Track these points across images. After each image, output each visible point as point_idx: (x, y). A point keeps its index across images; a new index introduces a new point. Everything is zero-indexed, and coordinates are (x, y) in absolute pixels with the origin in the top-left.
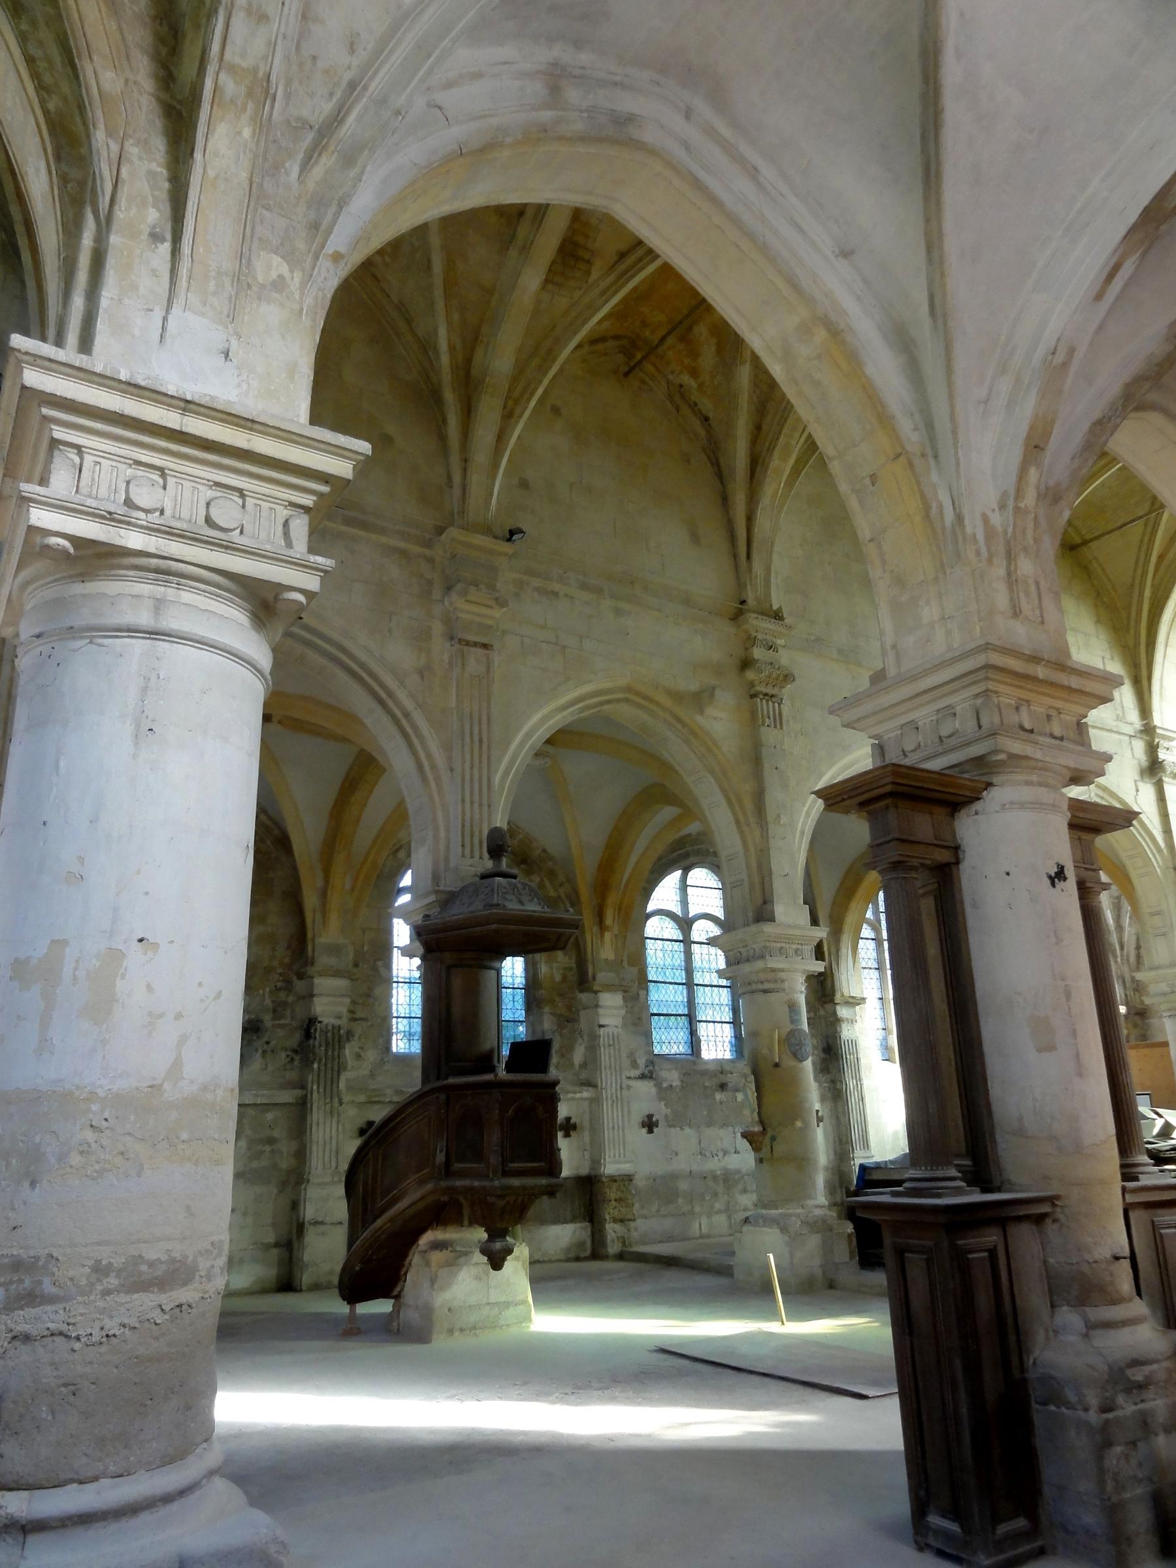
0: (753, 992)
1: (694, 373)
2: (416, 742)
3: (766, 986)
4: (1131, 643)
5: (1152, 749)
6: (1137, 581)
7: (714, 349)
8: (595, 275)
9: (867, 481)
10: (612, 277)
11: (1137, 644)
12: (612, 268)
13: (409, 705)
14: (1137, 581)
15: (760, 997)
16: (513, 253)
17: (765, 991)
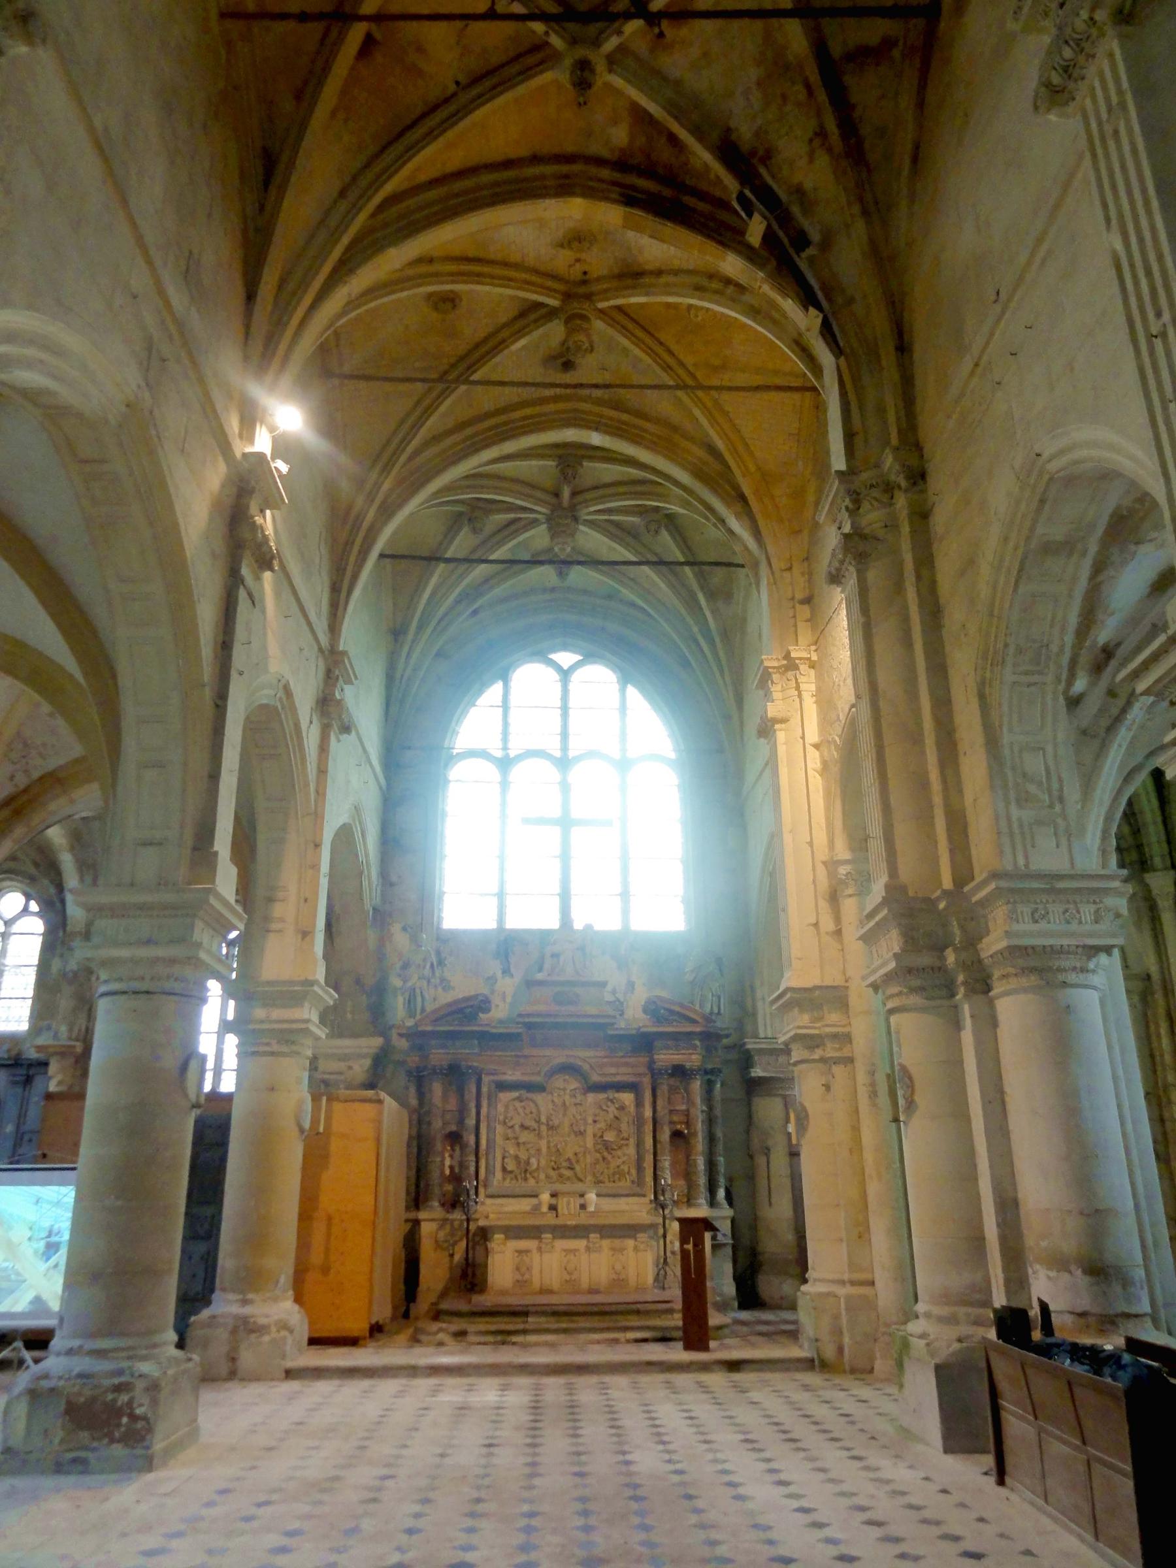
5: (330, 678)
11: (349, 543)
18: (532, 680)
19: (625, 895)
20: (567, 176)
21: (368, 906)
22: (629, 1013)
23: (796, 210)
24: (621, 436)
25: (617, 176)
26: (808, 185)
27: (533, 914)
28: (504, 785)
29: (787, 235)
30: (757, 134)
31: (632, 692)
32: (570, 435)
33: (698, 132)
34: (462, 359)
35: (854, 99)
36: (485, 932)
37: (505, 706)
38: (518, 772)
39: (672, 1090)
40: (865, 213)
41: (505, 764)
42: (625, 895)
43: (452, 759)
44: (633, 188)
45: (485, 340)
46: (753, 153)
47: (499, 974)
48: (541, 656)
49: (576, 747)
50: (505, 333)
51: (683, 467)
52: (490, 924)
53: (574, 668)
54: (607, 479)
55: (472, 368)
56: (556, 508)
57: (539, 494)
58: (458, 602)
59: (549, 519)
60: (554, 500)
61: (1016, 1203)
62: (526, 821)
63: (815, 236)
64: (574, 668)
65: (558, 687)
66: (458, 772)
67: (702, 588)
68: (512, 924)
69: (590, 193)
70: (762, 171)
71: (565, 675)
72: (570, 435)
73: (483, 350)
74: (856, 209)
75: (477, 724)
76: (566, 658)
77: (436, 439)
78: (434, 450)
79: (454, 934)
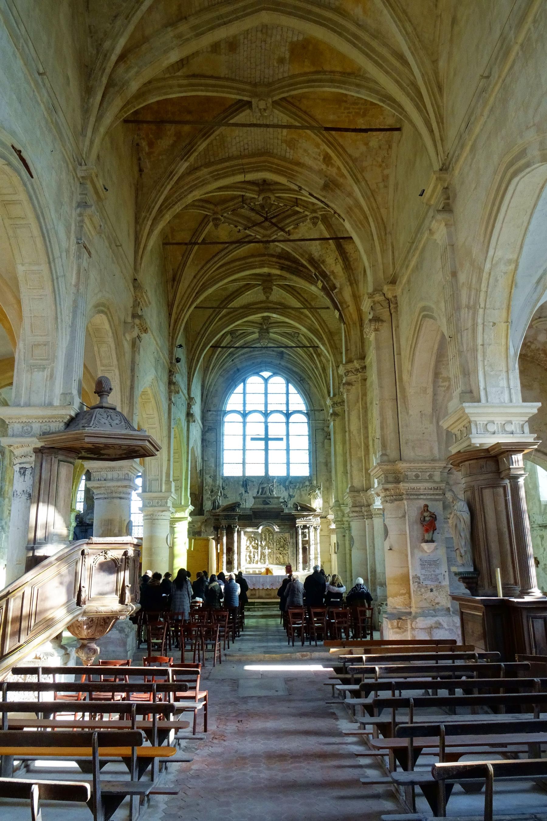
0: (113, 498)
1: (151, 144)
2: (57, 296)
3: (122, 495)
4: (190, 357)
6: (202, 332)
7: (171, 142)
8: (179, 74)
9: (491, 324)
10: (185, 82)
11: (193, 359)
12: (188, 77)
13: (60, 272)
14: (202, 332)
15: (117, 501)
16: (170, 33)
17: (121, 498)
18: (254, 383)
19: (288, 464)
20: (263, 261)
21: (198, 471)
22: (289, 506)
23: (332, 277)
24: (283, 316)
25: (278, 260)
26: (335, 271)
27: (255, 470)
28: (244, 423)
29: (329, 286)
30: (320, 256)
31: (291, 386)
32: (266, 314)
33: (302, 256)
34: (229, 296)
35: (347, 251)
36: (238, 477)
37: (244, 393)
38: (249, 418)
39: (303, 533)
40: (351, 284)
41: (244, 415)
42: (288, 464)
43: (225, 413)
44: (283, 264)
45: (237, 290)
46: (319, 260)
47: (244, 492)
48: (257, 374)
49: (270, 408)
50: (243, 289)
51: (304, 327)
52: (241, 474)
53: (270, 377)
54: (279, 320)
55: (232, 300)
56: (261, 329)
57: (256, 325)
58: (228, 356)
59: (259, 332)
60: (260, 326)
61: (375, 571)
62: (253, 439)
63: (338, 285)
64: (270, 377)
65: (263, 385)
66: (227, 418)
67: (315, 353)
68: (248, 474)
69: (270, 266)
70: (322, 266)
71: (266, 380)
72: (266, 314)
73: (236, 294)
74: (348, 284)
75: (234, 401)
76: (266, 374)
77: (220, 319)
78: (220, 323)
79: (228, 478)
